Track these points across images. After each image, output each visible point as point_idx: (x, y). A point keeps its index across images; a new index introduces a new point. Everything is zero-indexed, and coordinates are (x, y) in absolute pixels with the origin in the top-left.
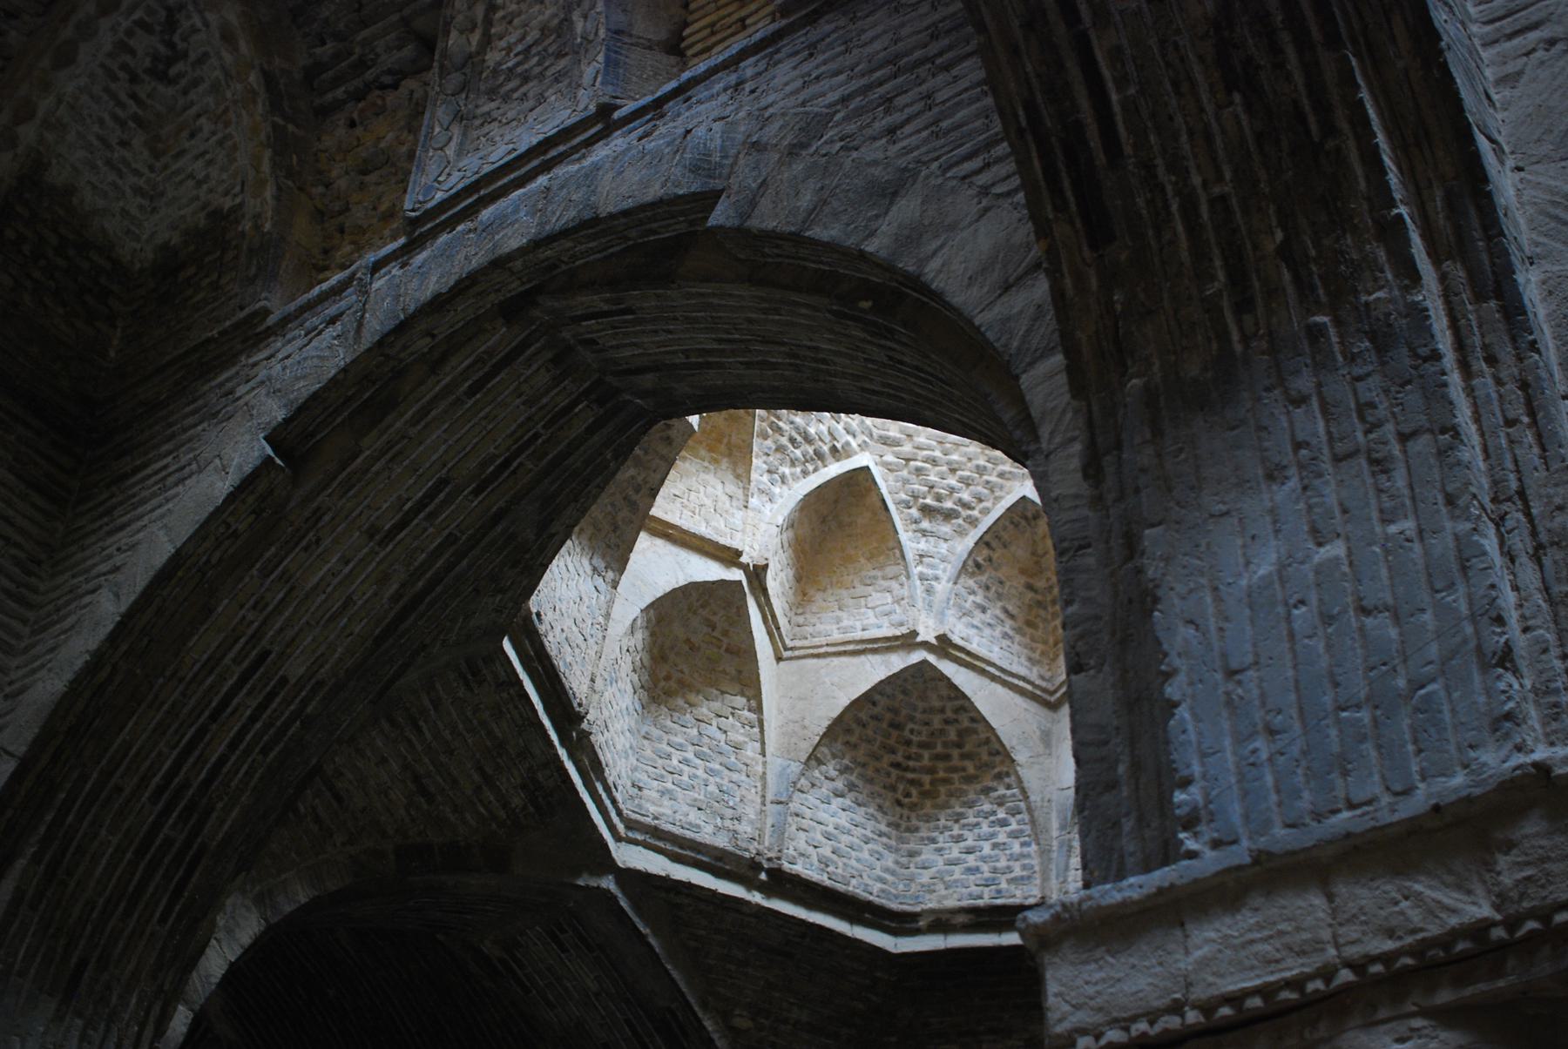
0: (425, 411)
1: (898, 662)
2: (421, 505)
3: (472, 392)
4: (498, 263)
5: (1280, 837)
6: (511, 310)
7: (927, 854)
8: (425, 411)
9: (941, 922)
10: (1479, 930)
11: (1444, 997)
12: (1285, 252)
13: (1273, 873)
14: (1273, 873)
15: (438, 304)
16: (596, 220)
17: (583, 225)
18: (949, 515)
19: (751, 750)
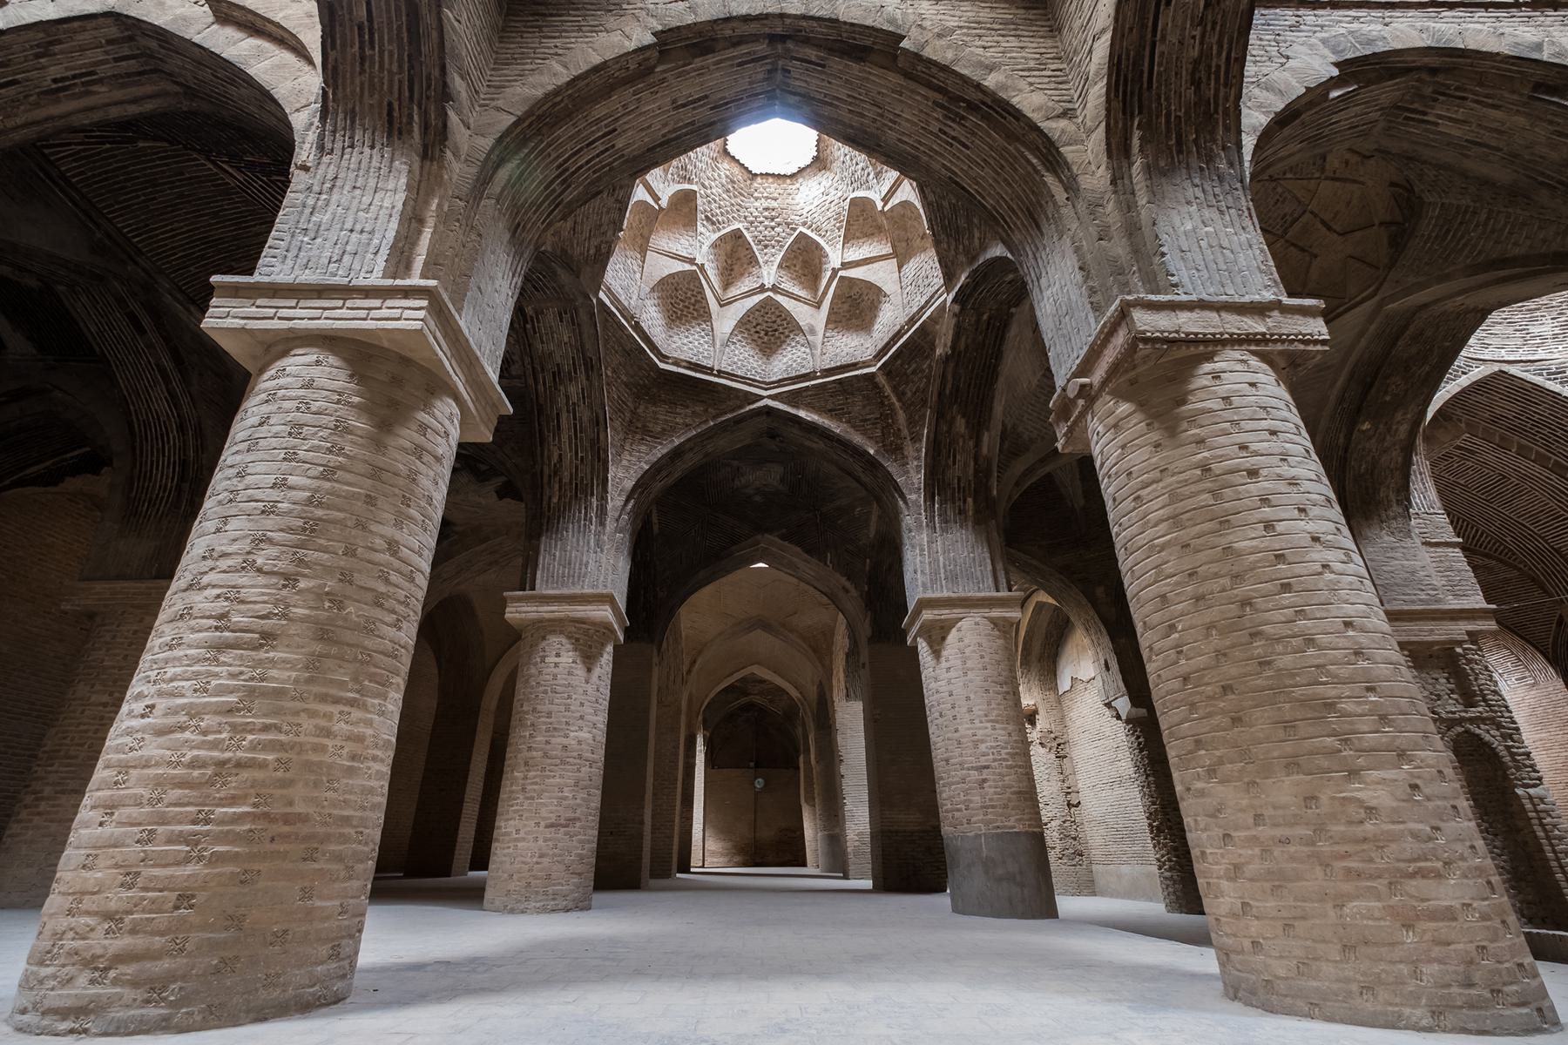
0: (721, 61)
1: (687, 267)
2: (694, 102)
3: (739, 65)
4: (782, 16)
5: (1205, 296)
6: (773, 39)
7: (676, 338)
8: (721, 61)
9: (677, 363)
10: (1264, 334)
11: (1253, 348)
12: (1195, 141)
13: (1202, 305)
14: (1202, 305)
15: (746, 19)
16: (837, 21)
17: (830, 20)
18: (713, 223)
19: (638, 276)
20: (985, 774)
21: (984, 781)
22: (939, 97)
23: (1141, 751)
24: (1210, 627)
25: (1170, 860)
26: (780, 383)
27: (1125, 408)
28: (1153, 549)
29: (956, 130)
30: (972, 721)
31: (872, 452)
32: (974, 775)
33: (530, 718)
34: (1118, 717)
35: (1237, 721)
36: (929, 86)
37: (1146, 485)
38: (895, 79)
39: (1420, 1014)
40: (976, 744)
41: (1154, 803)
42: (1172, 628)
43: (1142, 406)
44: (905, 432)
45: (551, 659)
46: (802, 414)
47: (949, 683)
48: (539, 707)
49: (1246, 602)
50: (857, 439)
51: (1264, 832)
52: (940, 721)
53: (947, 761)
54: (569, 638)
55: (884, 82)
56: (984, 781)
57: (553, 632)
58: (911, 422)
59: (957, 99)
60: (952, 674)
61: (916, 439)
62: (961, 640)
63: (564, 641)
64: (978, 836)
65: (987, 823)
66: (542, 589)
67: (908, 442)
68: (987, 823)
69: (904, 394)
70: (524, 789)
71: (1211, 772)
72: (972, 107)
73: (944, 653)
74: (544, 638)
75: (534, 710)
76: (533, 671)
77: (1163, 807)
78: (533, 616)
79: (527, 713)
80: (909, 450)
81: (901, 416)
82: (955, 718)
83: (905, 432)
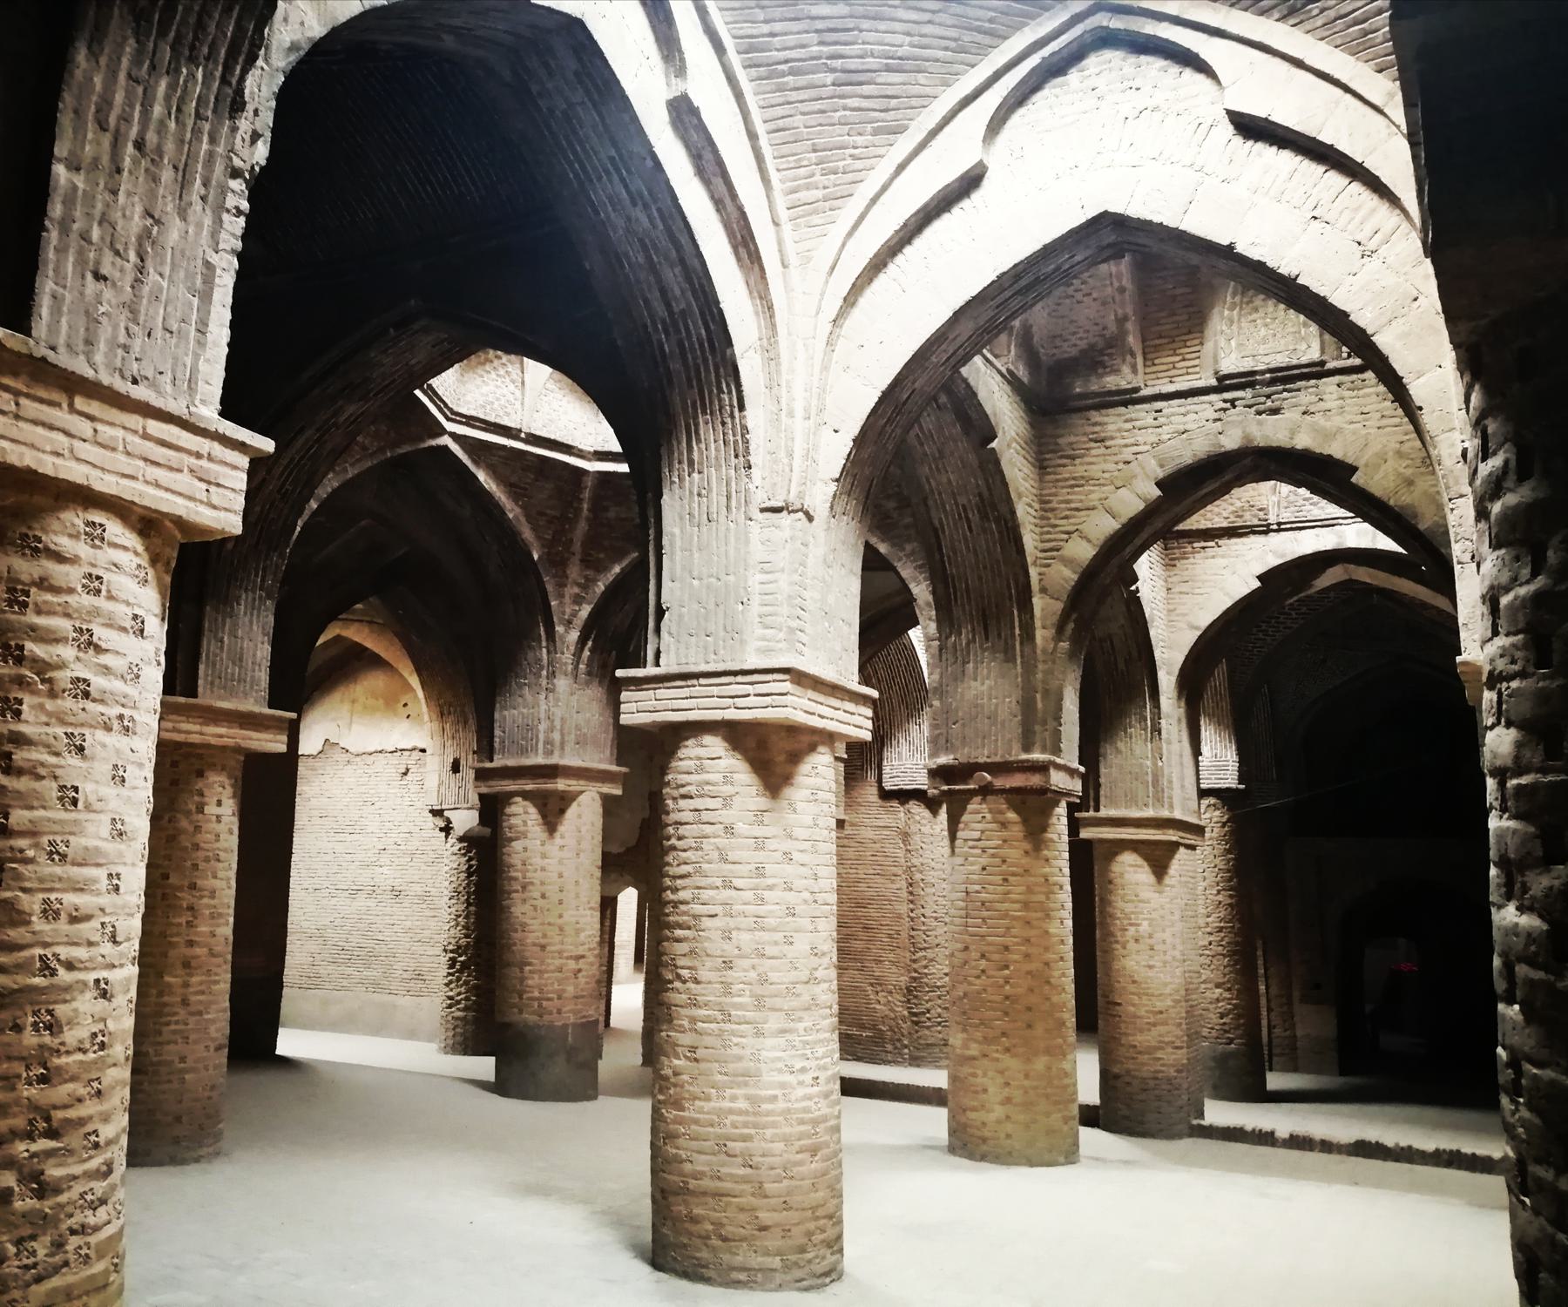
20: (582, 964)
21: (580, 971)
22: (986, 494)
23: (469, 874)
24: (1029, 973)
25: (467, 999)
26: (470, 421)
27: (1012, 816)
28: (1005, 916)
29: (974, 517)
30: (577, 908)
31: (536, 557)
32: (572, 965)
33: (186, 898)
34: (447, 830)
35: (1029, 1026)
36: (986, 481)
37: (1014, 874)
38: (972, 458)
39: (1062, 1159)
40: (578, 932)
41: (467, 936)
42: (1007, 967)
43: (1025, 821)
44: (577, 547)
45: (211, 809)
46: (482, 476)
47: (560, 862)
48: (199, 882)
49: (1047, 964)
50: (527, 533)
51: (1026, 1083)
52: (540, 903)
53: (543, 947)
54: (230, 777)
55: (962, 448)
56: (580, 971)
57: (212, 766)
58: (591, 542)
59: (994, 507)
60: (566, 854)
61: (594, 565)
62: (579, 816)
63: (227, 782)
64: (565, 1026)
65: (575, 1012)
66: (205, 697)
67: (576, 559)
68: (575, 1012)
69: (606, 509)
70: (185, 1002)
71: (1007, 1050)
72: (997, 520)
73: (561, 829)
74: (200, 774)
75: (193, 886)
76: (184, 823)
77: (478, 940)
78: (195, 739)
79: (181, 889)
80: (574, 572)
81: (582, 527)
82: (561, 903)
83: (577, 547)
